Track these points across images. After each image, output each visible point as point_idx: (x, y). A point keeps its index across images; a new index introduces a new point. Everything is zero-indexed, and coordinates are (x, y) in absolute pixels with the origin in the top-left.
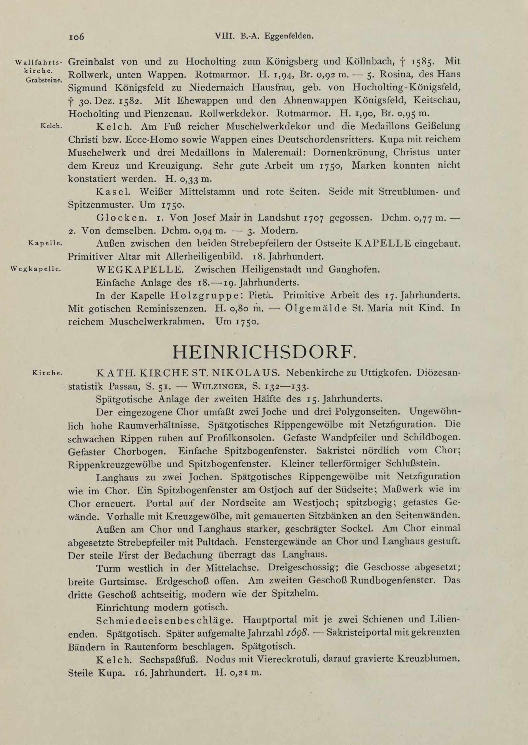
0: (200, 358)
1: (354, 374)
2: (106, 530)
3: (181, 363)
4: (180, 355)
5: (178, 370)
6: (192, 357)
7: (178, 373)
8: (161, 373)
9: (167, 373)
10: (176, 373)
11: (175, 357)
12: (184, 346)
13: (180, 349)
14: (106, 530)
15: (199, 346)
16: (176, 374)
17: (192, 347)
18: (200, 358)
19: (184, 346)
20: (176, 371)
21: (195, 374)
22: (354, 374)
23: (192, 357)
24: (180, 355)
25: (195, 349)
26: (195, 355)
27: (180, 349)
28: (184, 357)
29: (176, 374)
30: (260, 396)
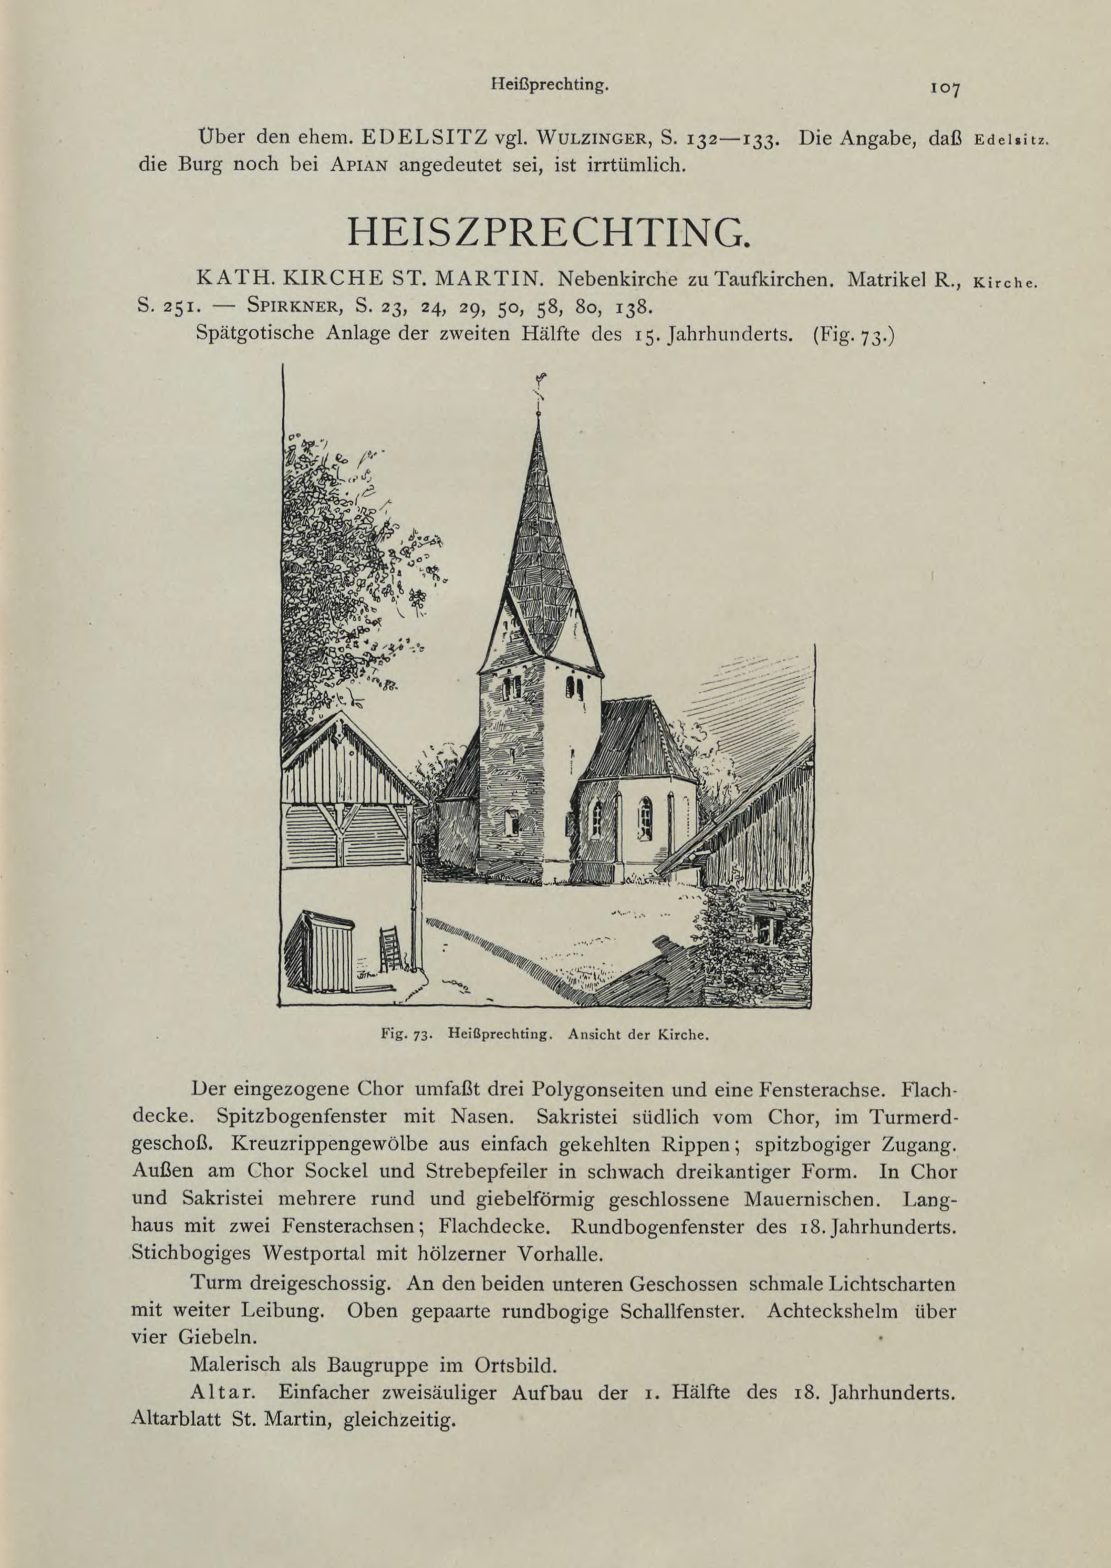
0: (405, 243)
1: (703, 281)
2: (154, 1171)
3: (364, 257)
4: (363, 238)
5: (361, 272)
6: (388, 243)
7: (352, 277)
8: (326, 278)
9: (338, 277)
10: (355, 277)
11: (353, 243)
12: (372, 220)
13: (363, 224)
14: (154, 1171)
15: (404, 219)
16: (356, 281)
17: (388, 220)
18: (405, 243)
19: (372, 220)
20: (356, 274)
21: (398, 281)
22: (703, 281)
23: (388, 243)
24: (363, 238)
25: (394, 225)
26: (395, 237)
27: (363, 224)
28: (372, 243)
29: (356, 281)
30: (535, 327)
